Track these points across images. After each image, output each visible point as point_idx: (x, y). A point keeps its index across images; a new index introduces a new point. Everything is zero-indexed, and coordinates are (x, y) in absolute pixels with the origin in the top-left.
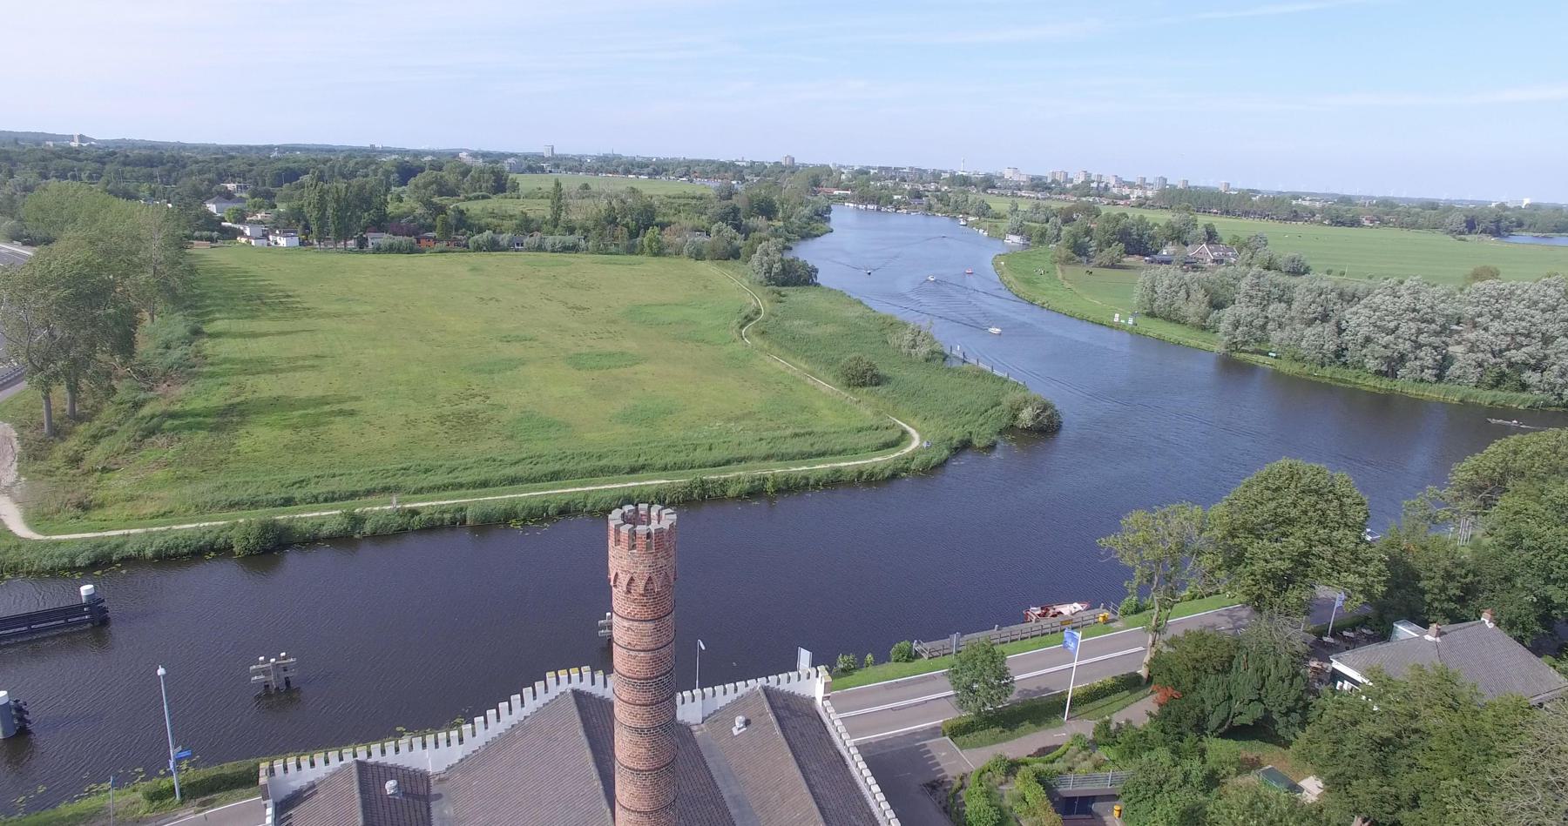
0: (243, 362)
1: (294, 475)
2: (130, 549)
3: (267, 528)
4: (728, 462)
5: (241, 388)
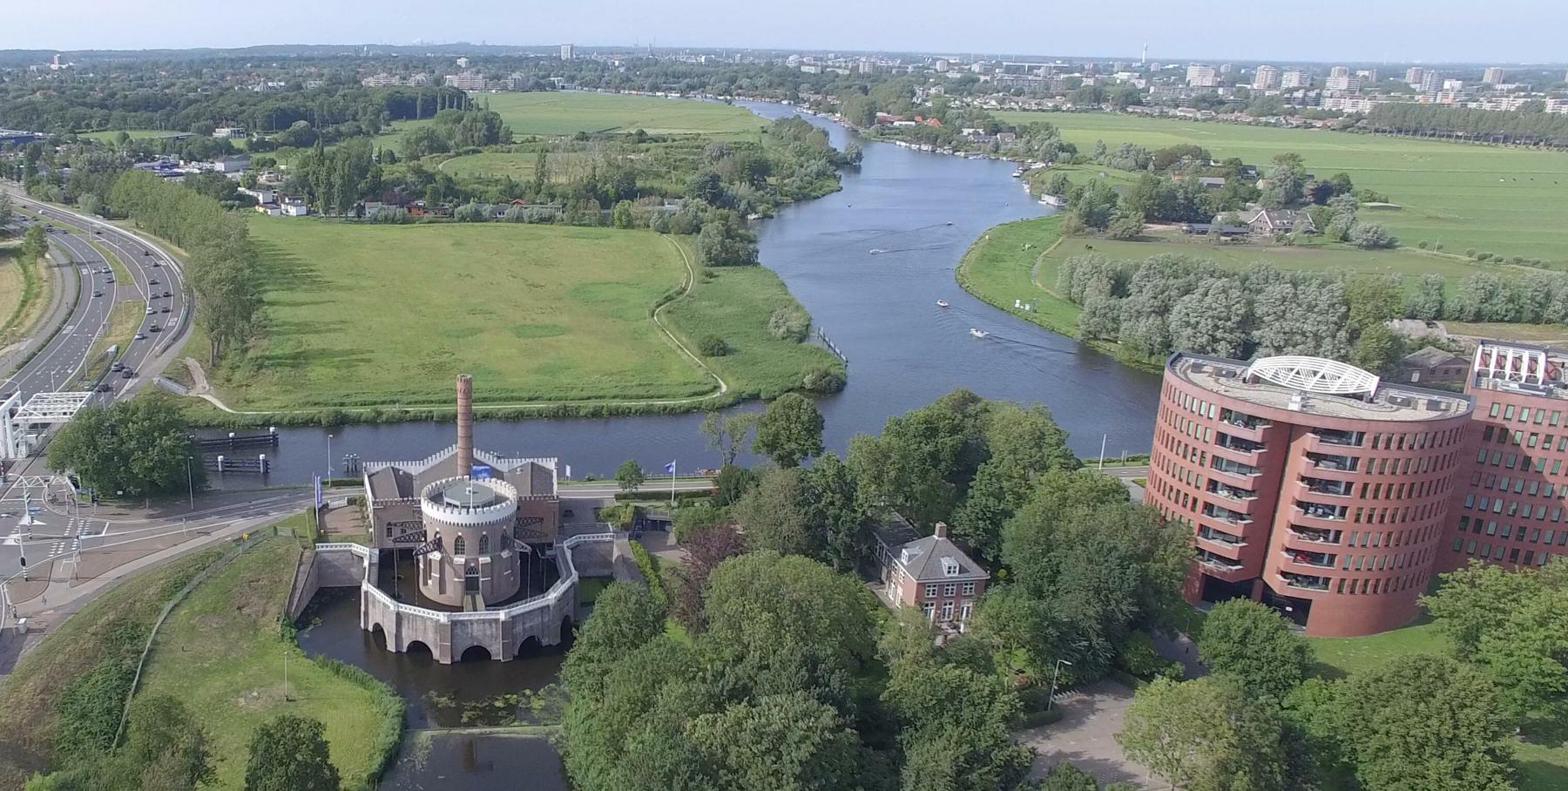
0: (296, 324)
1: (343, 392)
2: (277, 418)
3: (337, 413)
4: (589, 398)
5: (300, 343)
